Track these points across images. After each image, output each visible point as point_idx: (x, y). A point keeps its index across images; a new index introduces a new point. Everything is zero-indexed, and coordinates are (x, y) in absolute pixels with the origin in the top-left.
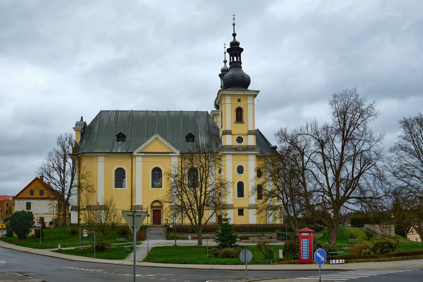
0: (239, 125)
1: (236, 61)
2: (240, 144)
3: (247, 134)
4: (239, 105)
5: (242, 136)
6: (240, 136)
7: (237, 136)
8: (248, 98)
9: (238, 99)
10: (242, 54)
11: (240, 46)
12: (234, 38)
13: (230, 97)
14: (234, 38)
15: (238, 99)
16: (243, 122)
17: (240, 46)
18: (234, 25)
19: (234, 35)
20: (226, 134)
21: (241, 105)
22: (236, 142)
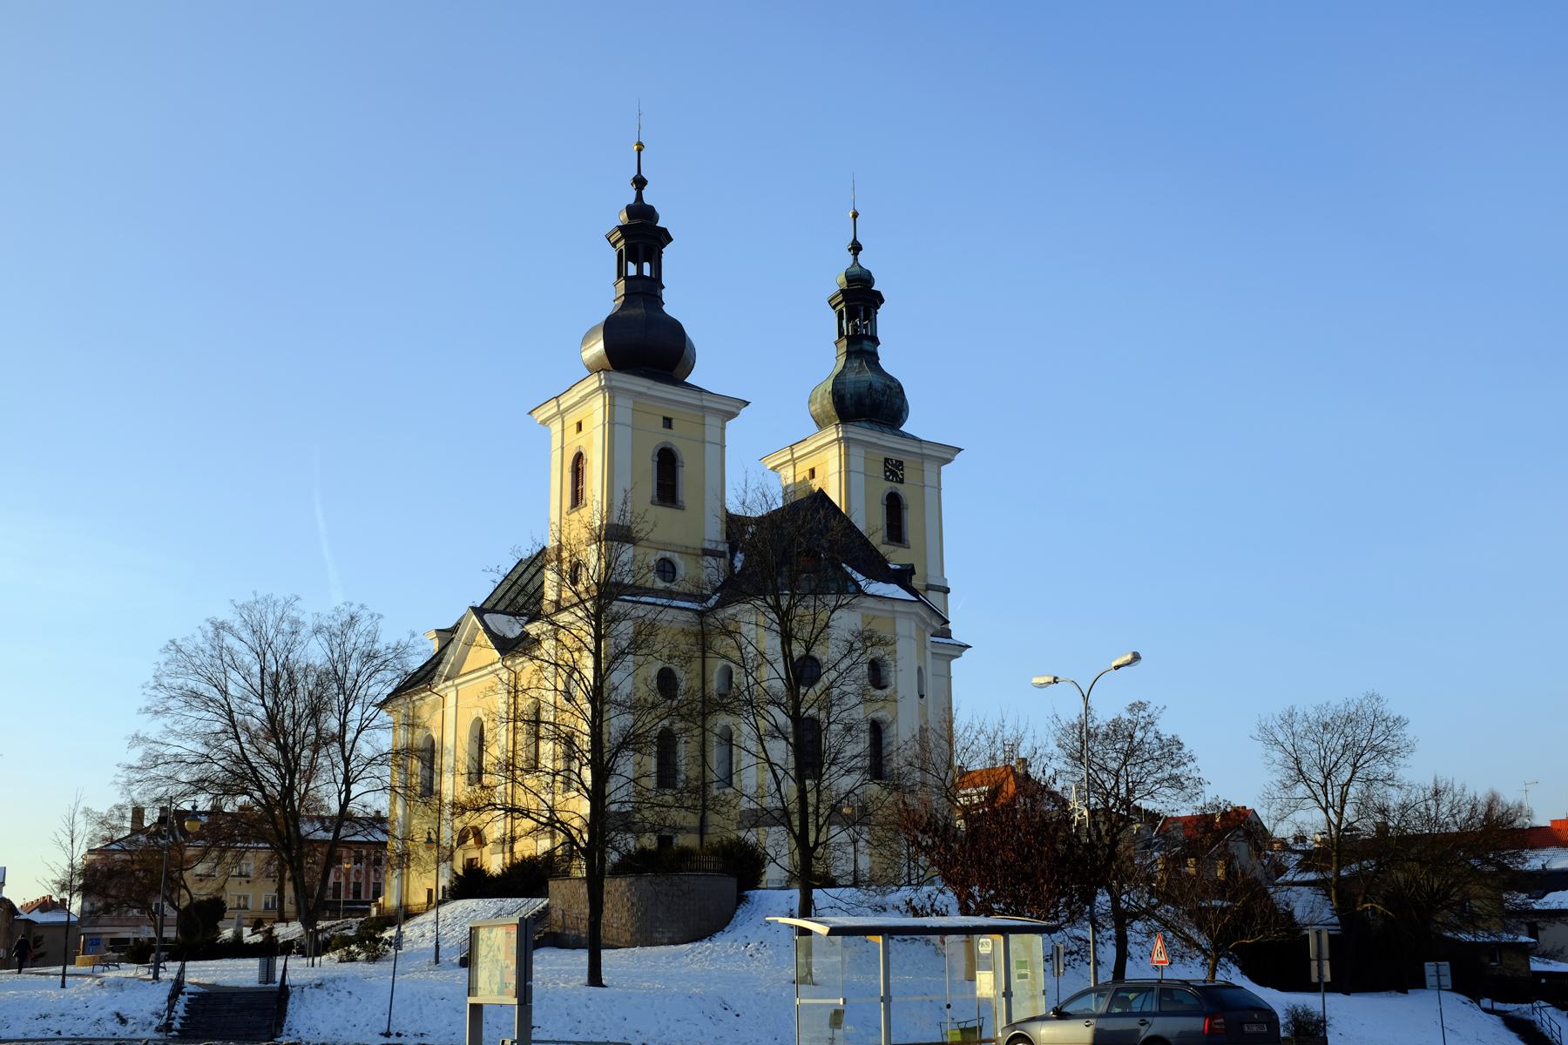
0: (666, 513)
1: (649, 275)
2: (668, 585)
4: (661, 437)
5: (676, 558)
6: (668, 555)
7: (661, 554)
9: (665, 418)
10: (668, 253)
12: (639, 197)
14: (639, 197)
15: (665, 418)
16: (680, 504)
18: (640, 147)
19: (640, 182)
21: (676, 440)
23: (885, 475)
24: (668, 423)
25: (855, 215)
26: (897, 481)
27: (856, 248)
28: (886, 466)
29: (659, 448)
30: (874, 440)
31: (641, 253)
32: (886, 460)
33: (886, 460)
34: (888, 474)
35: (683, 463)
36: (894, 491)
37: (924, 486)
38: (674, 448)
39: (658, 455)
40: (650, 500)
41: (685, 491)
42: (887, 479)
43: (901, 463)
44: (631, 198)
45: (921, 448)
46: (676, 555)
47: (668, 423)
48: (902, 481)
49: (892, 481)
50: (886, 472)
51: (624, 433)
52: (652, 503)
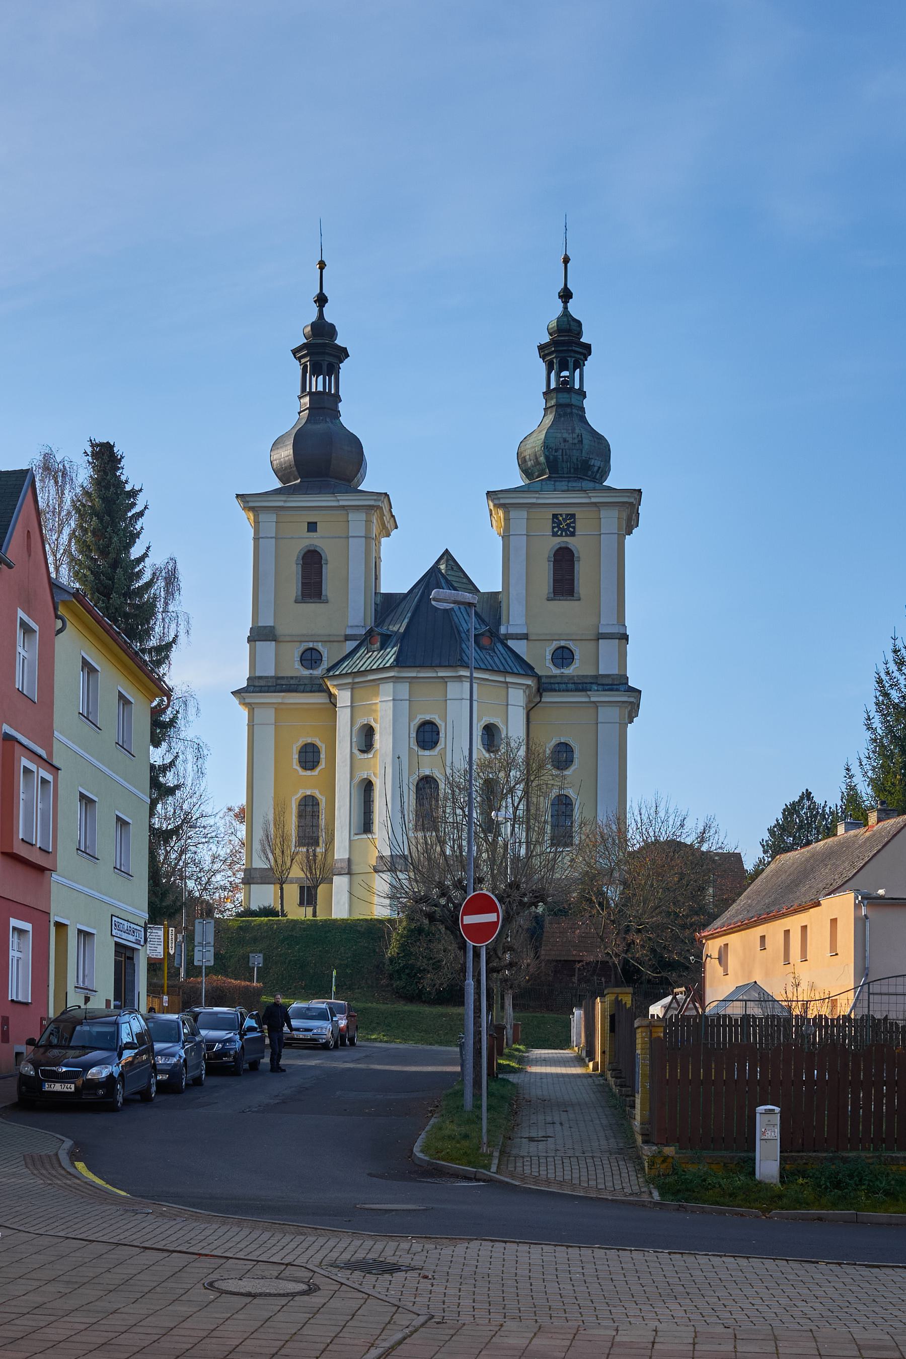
2: (311, 671)
3: (342, 639)
5: (319, 646)
8: (352, 516)
11: (339, 342)
13: (274, 518)
17: (339, 342)
20: (255, 641)
22: (297, 665)
23: (553, 531)
24: (312, 527)
25: (566, 260)
26: (567, 535)
27: (566, 295)
28: (553, 522)
29: (303, 553)
30: (534, 501)
31: (325, 368)
32: (555, 516)
33: (555, 516)
34: (556, 530)
35: (327, 560)
36: (563, 545)
37: (600, 535)
38: (318, 549)
39: (303, 558)
40: (293, 599)
41: (329, 587)
42: (555, 534)
43: (573, 516)
44: (313, 316)
45: (590, 497)
46: (320, 644)
47: (312, 527)
48: (573, 534)
49: (561, 535)
50: (553, 528)
51: (269, 546)
52: (296, 602)
